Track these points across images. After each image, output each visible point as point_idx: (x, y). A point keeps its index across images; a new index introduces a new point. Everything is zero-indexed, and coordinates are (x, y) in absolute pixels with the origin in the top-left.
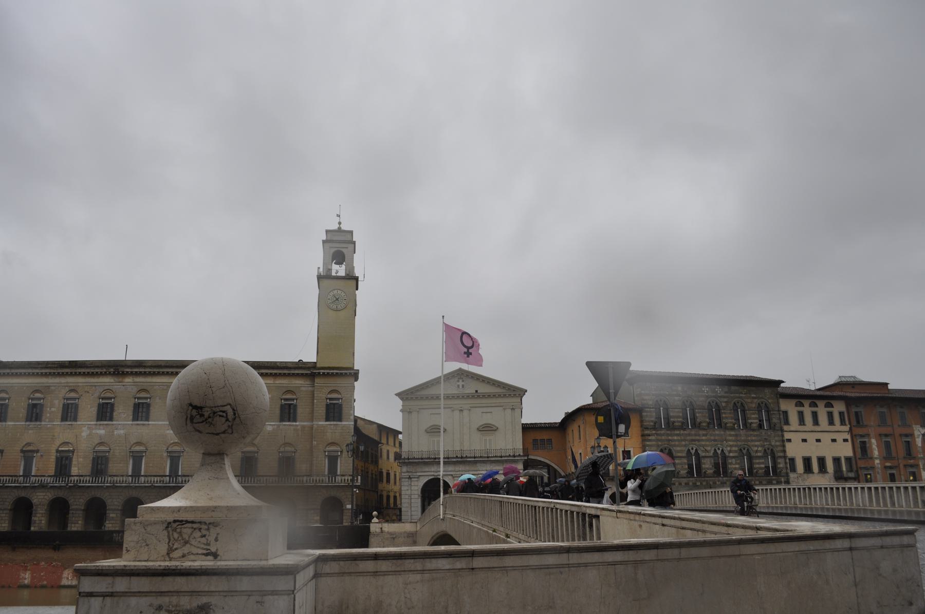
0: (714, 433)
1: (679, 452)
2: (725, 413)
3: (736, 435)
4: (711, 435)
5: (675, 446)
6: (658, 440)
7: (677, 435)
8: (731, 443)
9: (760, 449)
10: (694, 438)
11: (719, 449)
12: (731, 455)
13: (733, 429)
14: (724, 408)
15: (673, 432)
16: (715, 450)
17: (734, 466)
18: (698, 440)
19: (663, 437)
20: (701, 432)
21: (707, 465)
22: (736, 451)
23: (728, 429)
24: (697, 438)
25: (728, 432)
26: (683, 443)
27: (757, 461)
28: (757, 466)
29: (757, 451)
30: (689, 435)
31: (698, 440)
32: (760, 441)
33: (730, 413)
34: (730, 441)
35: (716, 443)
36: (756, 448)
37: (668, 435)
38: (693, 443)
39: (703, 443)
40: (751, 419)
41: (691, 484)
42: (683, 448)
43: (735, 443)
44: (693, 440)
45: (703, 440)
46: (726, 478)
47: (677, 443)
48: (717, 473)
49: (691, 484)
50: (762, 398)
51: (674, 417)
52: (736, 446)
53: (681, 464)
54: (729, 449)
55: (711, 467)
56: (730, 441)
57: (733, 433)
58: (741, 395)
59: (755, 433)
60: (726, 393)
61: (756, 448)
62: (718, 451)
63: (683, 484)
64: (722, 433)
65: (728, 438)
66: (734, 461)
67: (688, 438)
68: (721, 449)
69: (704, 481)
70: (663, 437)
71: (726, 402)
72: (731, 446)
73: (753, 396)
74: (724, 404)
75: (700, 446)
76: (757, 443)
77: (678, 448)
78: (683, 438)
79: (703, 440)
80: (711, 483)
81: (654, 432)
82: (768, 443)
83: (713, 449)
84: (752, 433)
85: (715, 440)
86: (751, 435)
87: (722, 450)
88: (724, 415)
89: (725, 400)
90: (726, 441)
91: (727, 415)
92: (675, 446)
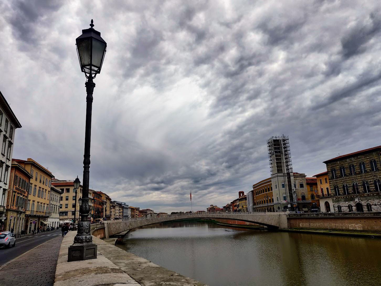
0: (352, 177)
1: (339, 186)
2: (356, 168)
3: (361, 176)
4: (351, 178)
5: (338, 184)
6: (333, 183)
7: (339, 180)
8: (359, 180)
9: (372, 180)
10: (344, 180)
11: (355, 183)
12: (359, 184)
13: (359, 174)
14: (356, 166)
15: (337, 179)
16: (353, 184)
17: (361, 189)
18: (346, 181)
19: (335, 182)
20: (347, 177)
21: (351, 190)
22: (361, 183)
23: (357, 174)
24: (346, 180)
25: (357, 176)
26: (341, 183)
27: (371, 186)
28: (371, 188)
29: (370, 182)
30: (343, 179)
31: (346, 181)
32: (371, 177)
33: (358, 168)
34: (358, 179)
35: (353, 181)
36: (370, 180)
37: (336, 181)
38: (345, 182)
39: (348, 182)
40: (367, 168)
41: (345, 197)
42: (341, 185)
43: (360, 180)
44: (345, 181)
45: (348, 180)
46: (358, 194)
47: (339, 183)
48: (354, 192)
49: (345, 197)
50: (372, 158)
51: (337, 174)
52: (361, 181)
53: (341, 190)
54: (358, 182)
55: (352, 190)
56: (358, 179)
57: (359, 175)
58: (362, 159)
59: (369, 174)
60: (356, 159)
61: (370, 180)
62: (354, 184)
63: (342, 198)
64: (355, 176)
65: (358, 178)
66: (360, 187)
67: (343, 180)
68: (356, 183)
69: (350, 196)
70: (335, 182)
71: (356, 163)
72: (359, 181)
73: (367, 158)
74: (355, 165)
75: (347, 183)
76: (370, 178)
77: (340, 185)
78: (341, 181)
79: (348, 180)
80: (352, 197)
81: (332, 180)
82: (376, 177)
83: (352, 183)
84: (367, 174)
85: (352, 180)
86: (367, 175)
87: (356, 183)
88: (355, 169)
89: (356, 162)
90: (357, 179)
91: (356, 169)
92: (338, 184)
